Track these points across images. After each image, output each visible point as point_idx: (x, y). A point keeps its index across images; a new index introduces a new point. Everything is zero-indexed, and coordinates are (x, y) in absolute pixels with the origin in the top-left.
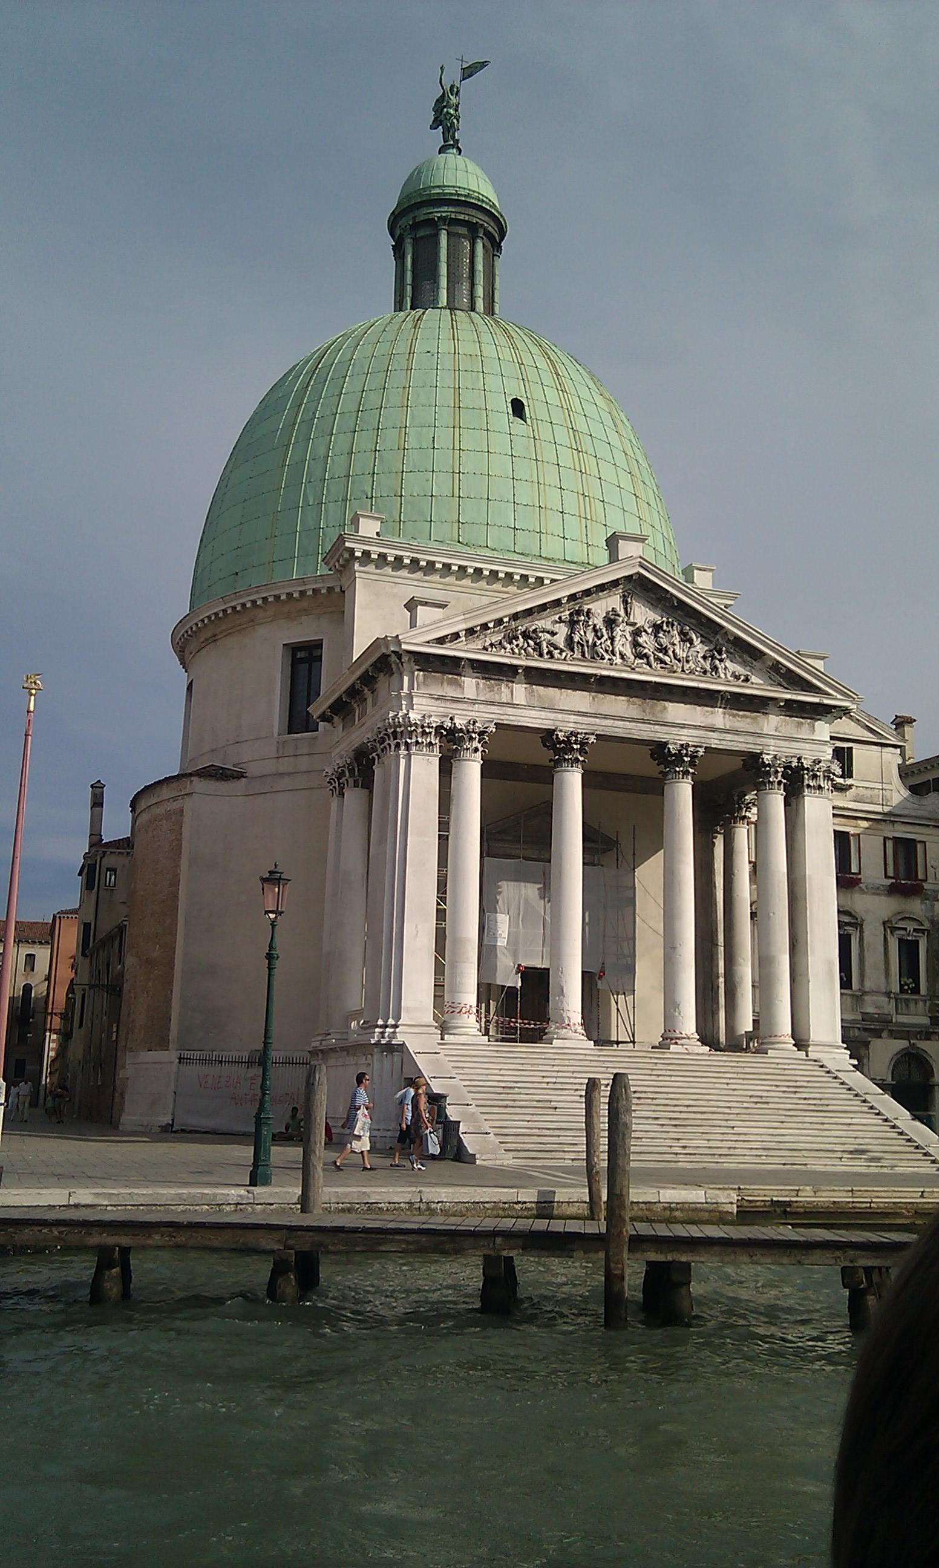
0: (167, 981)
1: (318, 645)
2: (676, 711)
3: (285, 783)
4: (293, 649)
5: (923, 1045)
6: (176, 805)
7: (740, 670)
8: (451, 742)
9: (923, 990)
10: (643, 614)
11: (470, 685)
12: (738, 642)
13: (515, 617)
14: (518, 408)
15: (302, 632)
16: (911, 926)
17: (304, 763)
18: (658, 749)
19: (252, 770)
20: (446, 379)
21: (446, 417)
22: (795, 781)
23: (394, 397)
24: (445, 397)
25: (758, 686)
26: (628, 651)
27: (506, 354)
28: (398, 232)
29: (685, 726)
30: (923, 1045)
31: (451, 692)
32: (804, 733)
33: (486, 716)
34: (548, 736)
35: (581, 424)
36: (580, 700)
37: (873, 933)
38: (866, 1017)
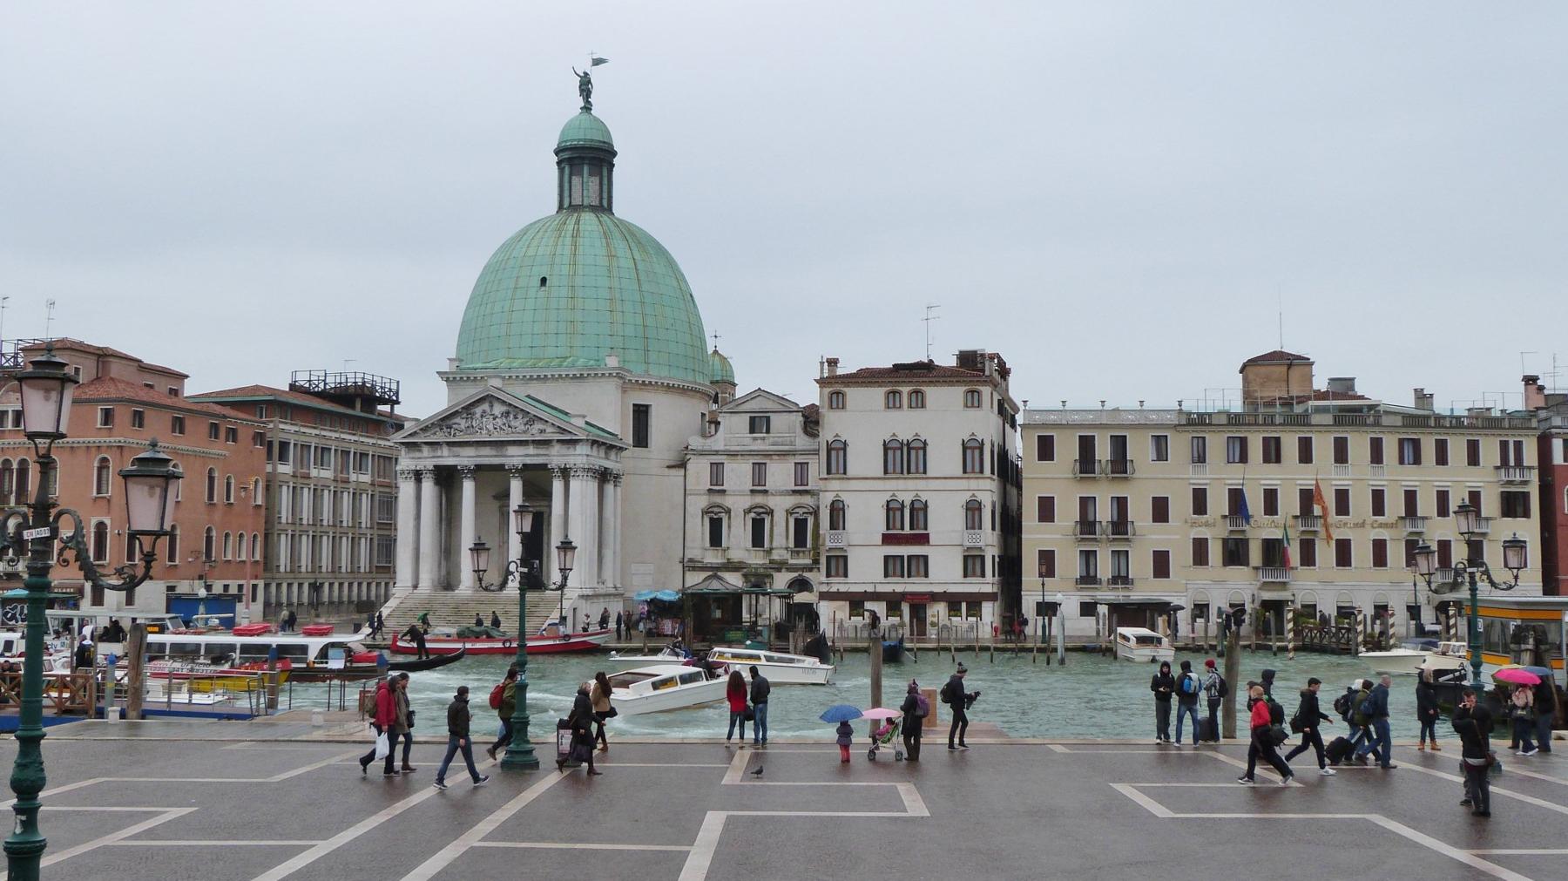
2: (512, 450)
5: (807, 575)
7: (541, 426)
8: (418, 476)
9: (809, 545)
10: (498, 409)
11: (426, 450)
13: (443, 419)
14: (544, 281)
16: (801, 511)
22: (565, 473)
25: (550, 434)
26: (491, 427)
29: (516, 457)
30: (807, 575)
31: (417, 454)
32: (571, 451)
33: (430, 464)
35: (579, 281)
36: (470, 451)
37: (780, 517)
38: (772, 562)
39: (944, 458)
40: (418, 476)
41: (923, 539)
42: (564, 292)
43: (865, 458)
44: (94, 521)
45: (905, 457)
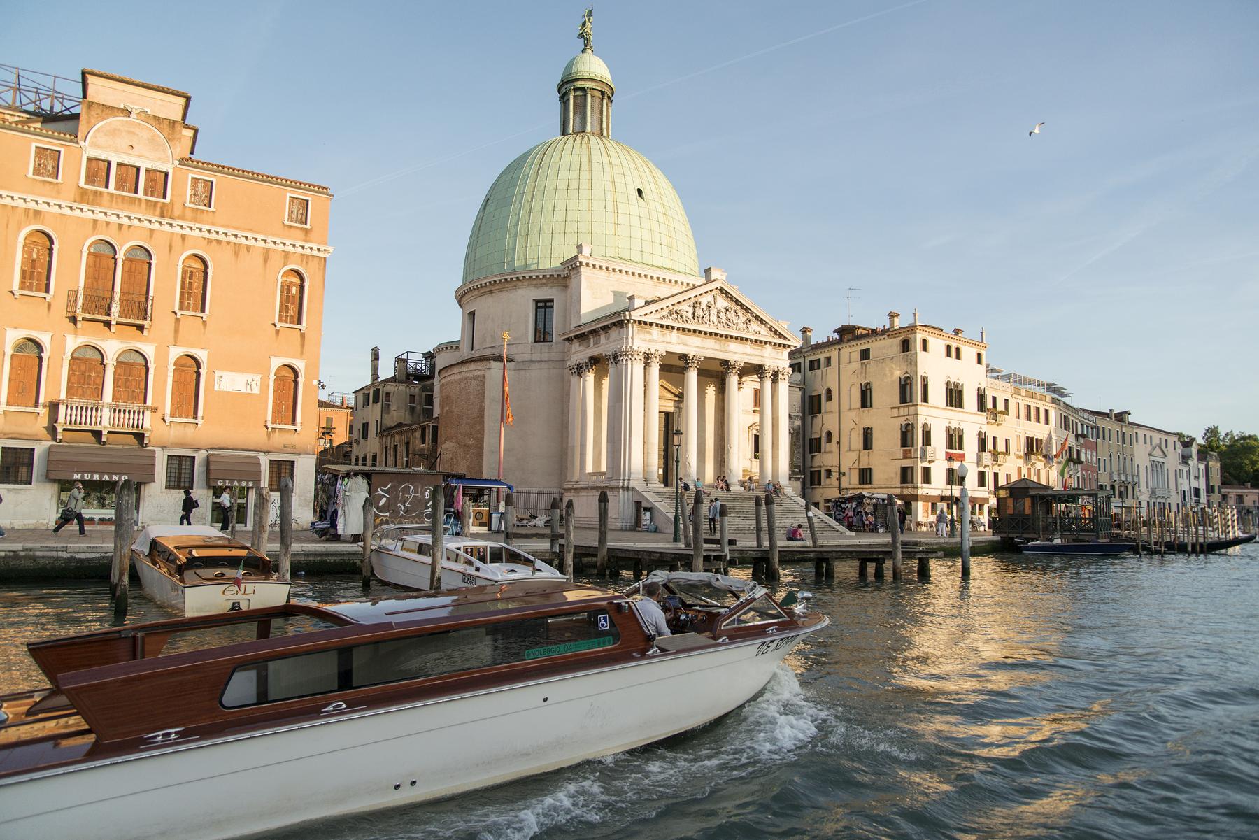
0: (480, 455)
1: (552, 301)
2: (733, 346)
3: (537, 365)
4: (537, 301)
6: (482, 373)
8: (648, 358)
10: (722, 303)
12: (757, 317)
14: (640, 192)
15: (543, 293)
17: (545, 357)
18: (725, 363)
19: (518, 358)
20: (608, 177)
21: (610, 196)
23: (585, 184)
24: (609, 186)
25: (765, 334)
27: (632, 165)
28: (563, 90)
29: (738, 354)
31: (648, 337)
32: (779, 356)
33: (662, 349)
34: (684, 357)
39: (970, 400)
40: (648, 358)
41: (962, 458)
42: (660, 208)
43: (938, 394)
44: (276, 362)
45: (954, 397)
